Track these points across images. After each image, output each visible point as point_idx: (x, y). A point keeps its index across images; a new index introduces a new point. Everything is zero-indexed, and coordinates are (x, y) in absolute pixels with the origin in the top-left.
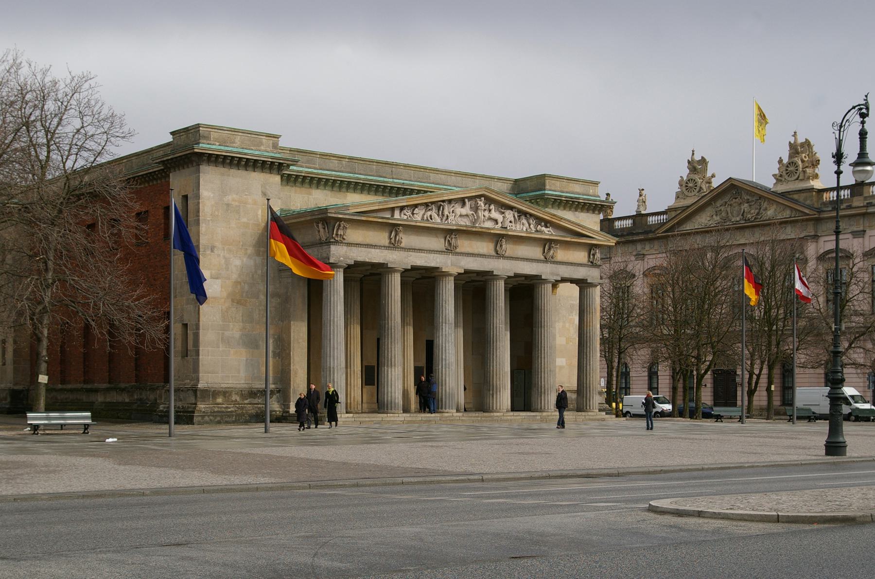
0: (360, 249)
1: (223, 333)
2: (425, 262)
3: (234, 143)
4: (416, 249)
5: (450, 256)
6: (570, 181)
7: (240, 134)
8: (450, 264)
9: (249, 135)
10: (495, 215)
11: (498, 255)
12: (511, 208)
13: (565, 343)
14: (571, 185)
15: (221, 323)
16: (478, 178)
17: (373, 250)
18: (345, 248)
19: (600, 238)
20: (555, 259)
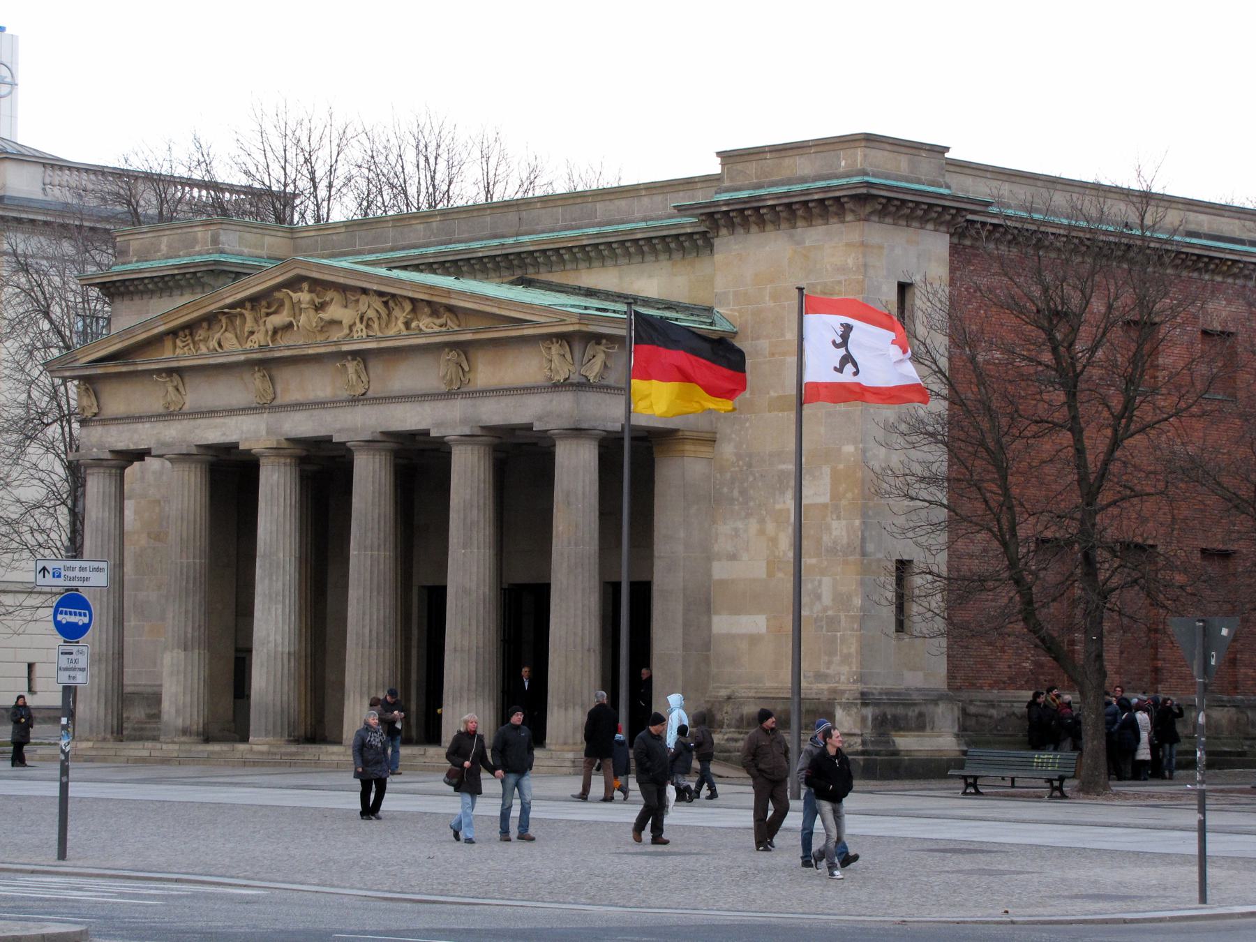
0: (121, 427)
1: (135, 595)
2: (224, 434)
3: (159, 251)
4: (203, 413)
5: (265, 415)
6: (783, 154)
7: (167, 232)
8: (264, 433)
9: (180, 231)
10: (335, 311)
11: (354, 400)
12: (365, 291)
13: (764, 576)
14: (787, 160)
15: (133, 577)
16: (699, 185)
17: (140, 426)
18: (99, 429)
19: (542, 320)
20: (471, 388)
